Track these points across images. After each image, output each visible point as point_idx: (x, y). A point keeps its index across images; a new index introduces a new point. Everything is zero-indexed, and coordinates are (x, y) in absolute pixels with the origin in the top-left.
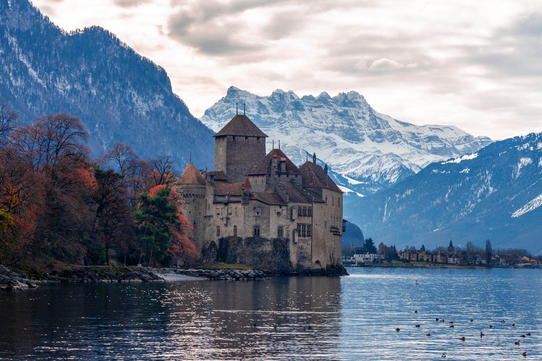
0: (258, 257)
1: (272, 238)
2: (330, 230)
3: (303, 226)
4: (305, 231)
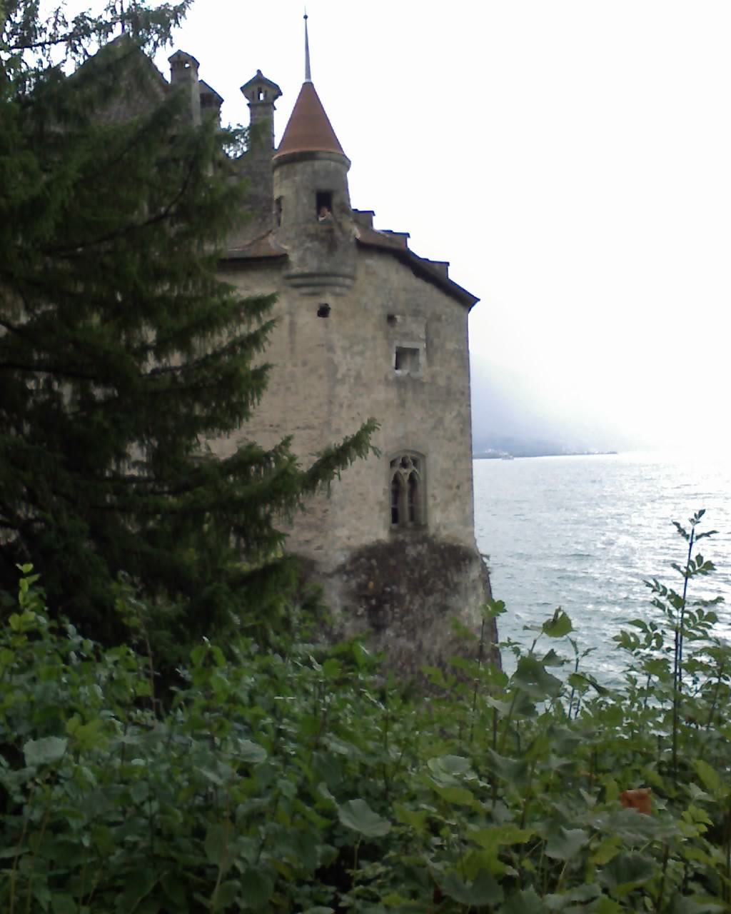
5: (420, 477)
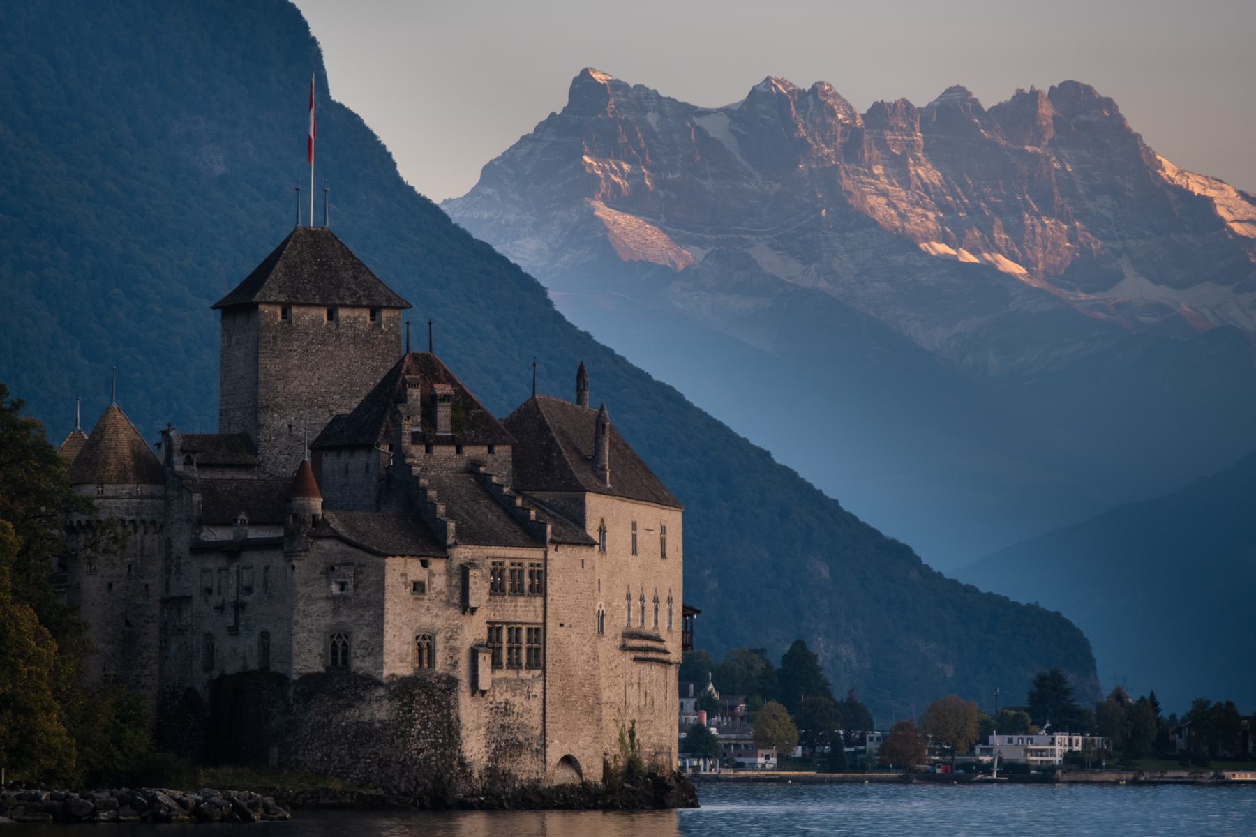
0: (344, 744)
1: (393, 675)
2: (618, 643)
3: (510, 630)
4: (519, 649)
5: (348, 644)
